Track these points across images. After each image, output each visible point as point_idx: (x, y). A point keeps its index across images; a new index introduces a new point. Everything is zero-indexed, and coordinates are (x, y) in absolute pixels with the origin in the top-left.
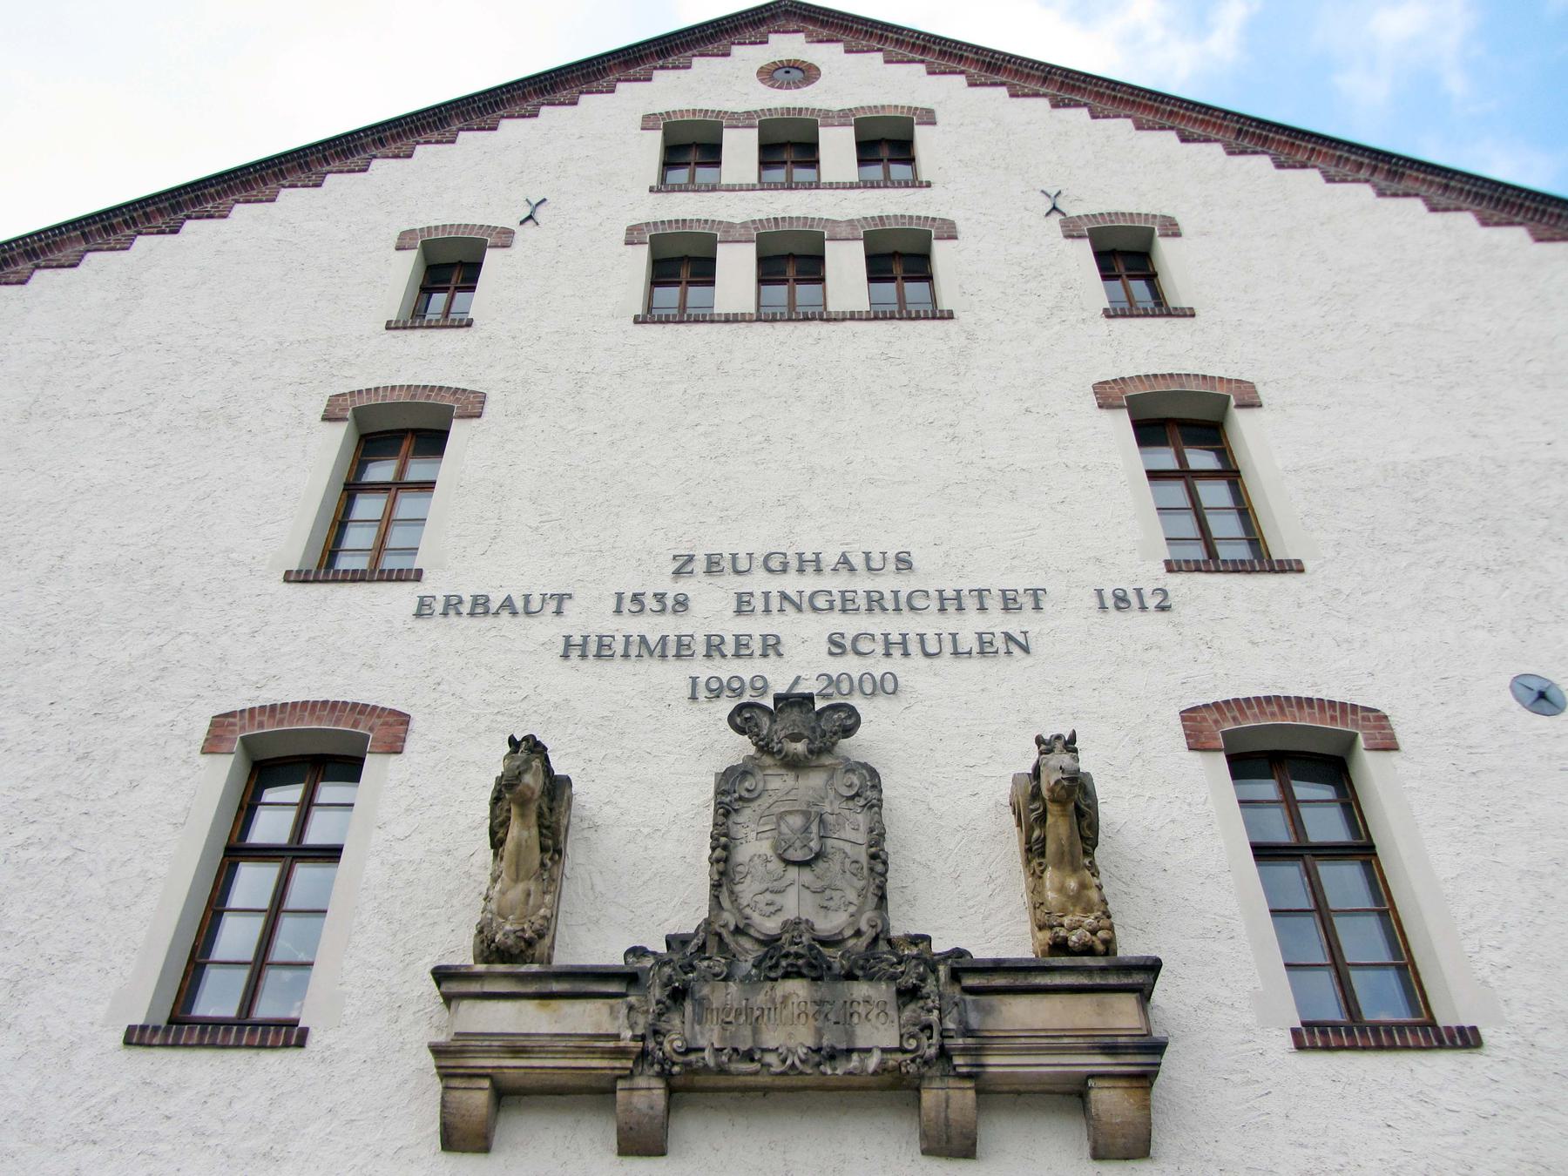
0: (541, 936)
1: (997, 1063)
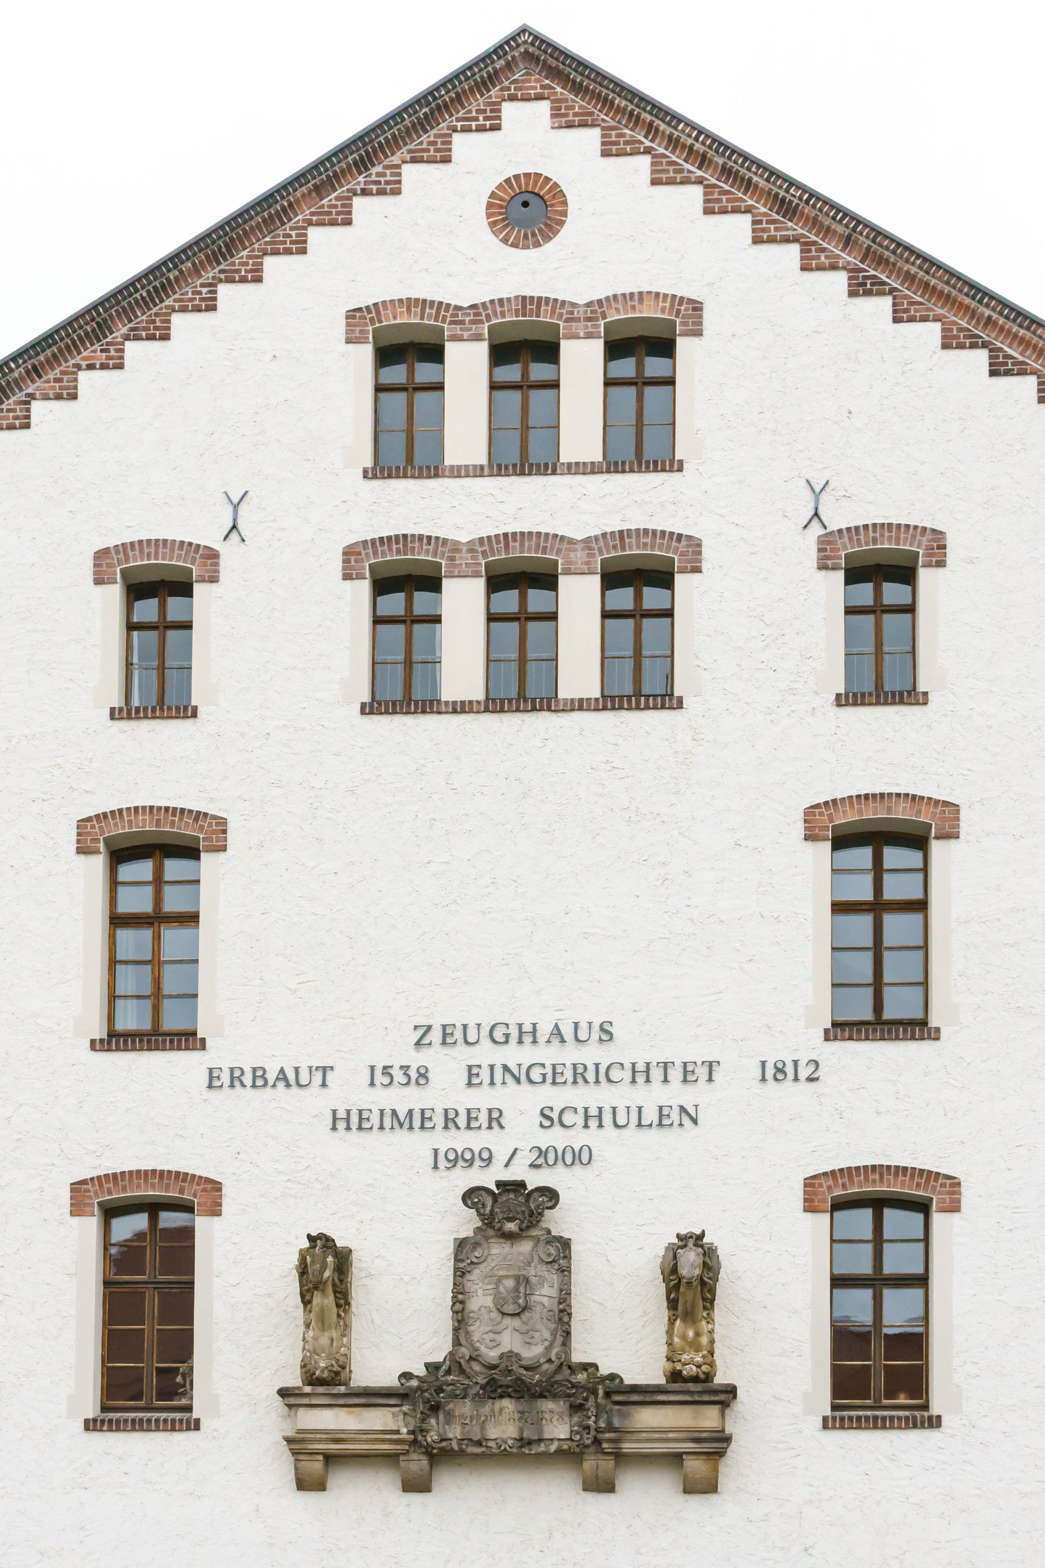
0: (344, 1368)
1: (628, 1447)
